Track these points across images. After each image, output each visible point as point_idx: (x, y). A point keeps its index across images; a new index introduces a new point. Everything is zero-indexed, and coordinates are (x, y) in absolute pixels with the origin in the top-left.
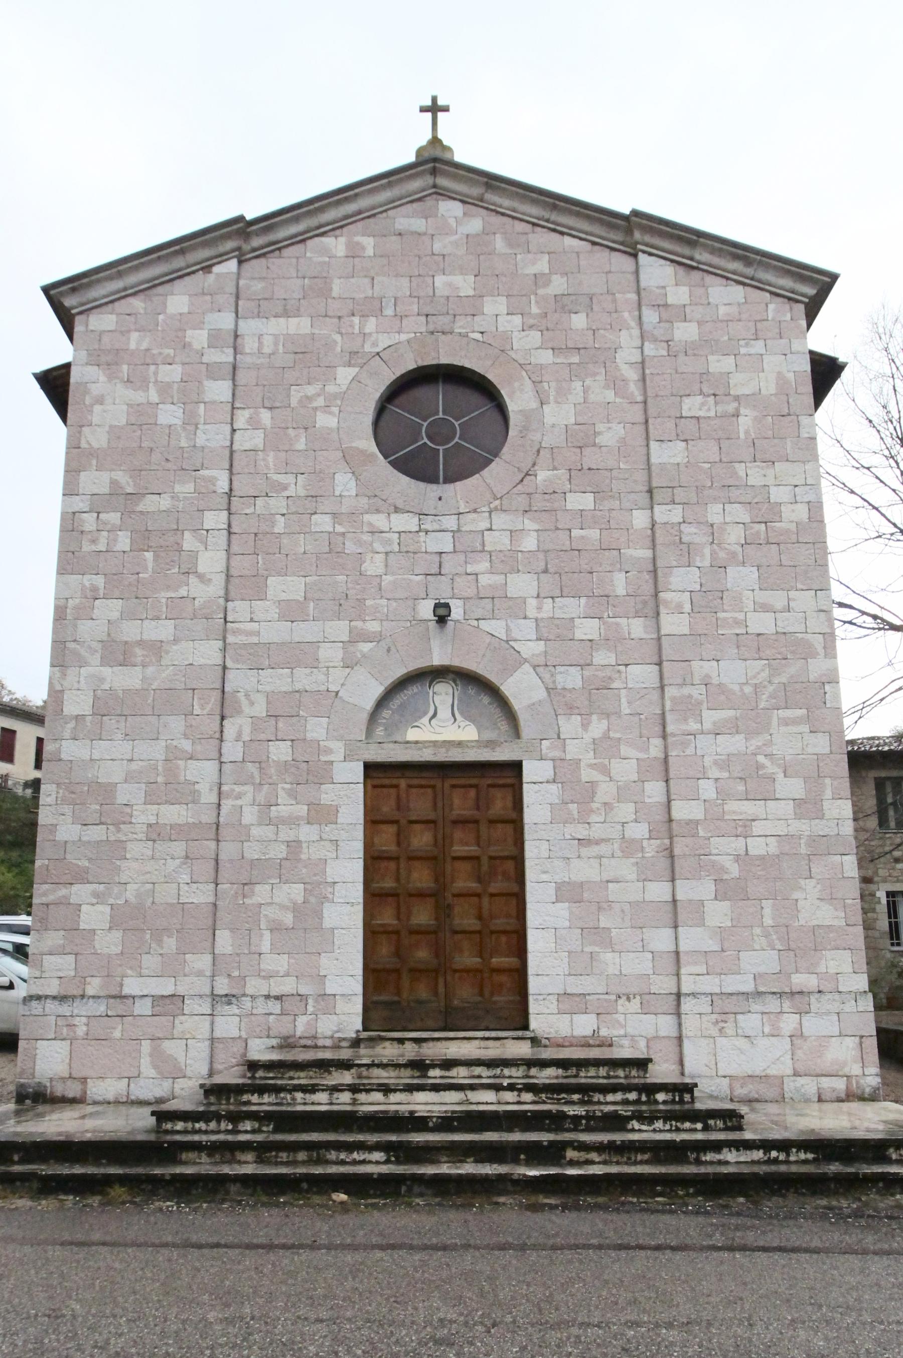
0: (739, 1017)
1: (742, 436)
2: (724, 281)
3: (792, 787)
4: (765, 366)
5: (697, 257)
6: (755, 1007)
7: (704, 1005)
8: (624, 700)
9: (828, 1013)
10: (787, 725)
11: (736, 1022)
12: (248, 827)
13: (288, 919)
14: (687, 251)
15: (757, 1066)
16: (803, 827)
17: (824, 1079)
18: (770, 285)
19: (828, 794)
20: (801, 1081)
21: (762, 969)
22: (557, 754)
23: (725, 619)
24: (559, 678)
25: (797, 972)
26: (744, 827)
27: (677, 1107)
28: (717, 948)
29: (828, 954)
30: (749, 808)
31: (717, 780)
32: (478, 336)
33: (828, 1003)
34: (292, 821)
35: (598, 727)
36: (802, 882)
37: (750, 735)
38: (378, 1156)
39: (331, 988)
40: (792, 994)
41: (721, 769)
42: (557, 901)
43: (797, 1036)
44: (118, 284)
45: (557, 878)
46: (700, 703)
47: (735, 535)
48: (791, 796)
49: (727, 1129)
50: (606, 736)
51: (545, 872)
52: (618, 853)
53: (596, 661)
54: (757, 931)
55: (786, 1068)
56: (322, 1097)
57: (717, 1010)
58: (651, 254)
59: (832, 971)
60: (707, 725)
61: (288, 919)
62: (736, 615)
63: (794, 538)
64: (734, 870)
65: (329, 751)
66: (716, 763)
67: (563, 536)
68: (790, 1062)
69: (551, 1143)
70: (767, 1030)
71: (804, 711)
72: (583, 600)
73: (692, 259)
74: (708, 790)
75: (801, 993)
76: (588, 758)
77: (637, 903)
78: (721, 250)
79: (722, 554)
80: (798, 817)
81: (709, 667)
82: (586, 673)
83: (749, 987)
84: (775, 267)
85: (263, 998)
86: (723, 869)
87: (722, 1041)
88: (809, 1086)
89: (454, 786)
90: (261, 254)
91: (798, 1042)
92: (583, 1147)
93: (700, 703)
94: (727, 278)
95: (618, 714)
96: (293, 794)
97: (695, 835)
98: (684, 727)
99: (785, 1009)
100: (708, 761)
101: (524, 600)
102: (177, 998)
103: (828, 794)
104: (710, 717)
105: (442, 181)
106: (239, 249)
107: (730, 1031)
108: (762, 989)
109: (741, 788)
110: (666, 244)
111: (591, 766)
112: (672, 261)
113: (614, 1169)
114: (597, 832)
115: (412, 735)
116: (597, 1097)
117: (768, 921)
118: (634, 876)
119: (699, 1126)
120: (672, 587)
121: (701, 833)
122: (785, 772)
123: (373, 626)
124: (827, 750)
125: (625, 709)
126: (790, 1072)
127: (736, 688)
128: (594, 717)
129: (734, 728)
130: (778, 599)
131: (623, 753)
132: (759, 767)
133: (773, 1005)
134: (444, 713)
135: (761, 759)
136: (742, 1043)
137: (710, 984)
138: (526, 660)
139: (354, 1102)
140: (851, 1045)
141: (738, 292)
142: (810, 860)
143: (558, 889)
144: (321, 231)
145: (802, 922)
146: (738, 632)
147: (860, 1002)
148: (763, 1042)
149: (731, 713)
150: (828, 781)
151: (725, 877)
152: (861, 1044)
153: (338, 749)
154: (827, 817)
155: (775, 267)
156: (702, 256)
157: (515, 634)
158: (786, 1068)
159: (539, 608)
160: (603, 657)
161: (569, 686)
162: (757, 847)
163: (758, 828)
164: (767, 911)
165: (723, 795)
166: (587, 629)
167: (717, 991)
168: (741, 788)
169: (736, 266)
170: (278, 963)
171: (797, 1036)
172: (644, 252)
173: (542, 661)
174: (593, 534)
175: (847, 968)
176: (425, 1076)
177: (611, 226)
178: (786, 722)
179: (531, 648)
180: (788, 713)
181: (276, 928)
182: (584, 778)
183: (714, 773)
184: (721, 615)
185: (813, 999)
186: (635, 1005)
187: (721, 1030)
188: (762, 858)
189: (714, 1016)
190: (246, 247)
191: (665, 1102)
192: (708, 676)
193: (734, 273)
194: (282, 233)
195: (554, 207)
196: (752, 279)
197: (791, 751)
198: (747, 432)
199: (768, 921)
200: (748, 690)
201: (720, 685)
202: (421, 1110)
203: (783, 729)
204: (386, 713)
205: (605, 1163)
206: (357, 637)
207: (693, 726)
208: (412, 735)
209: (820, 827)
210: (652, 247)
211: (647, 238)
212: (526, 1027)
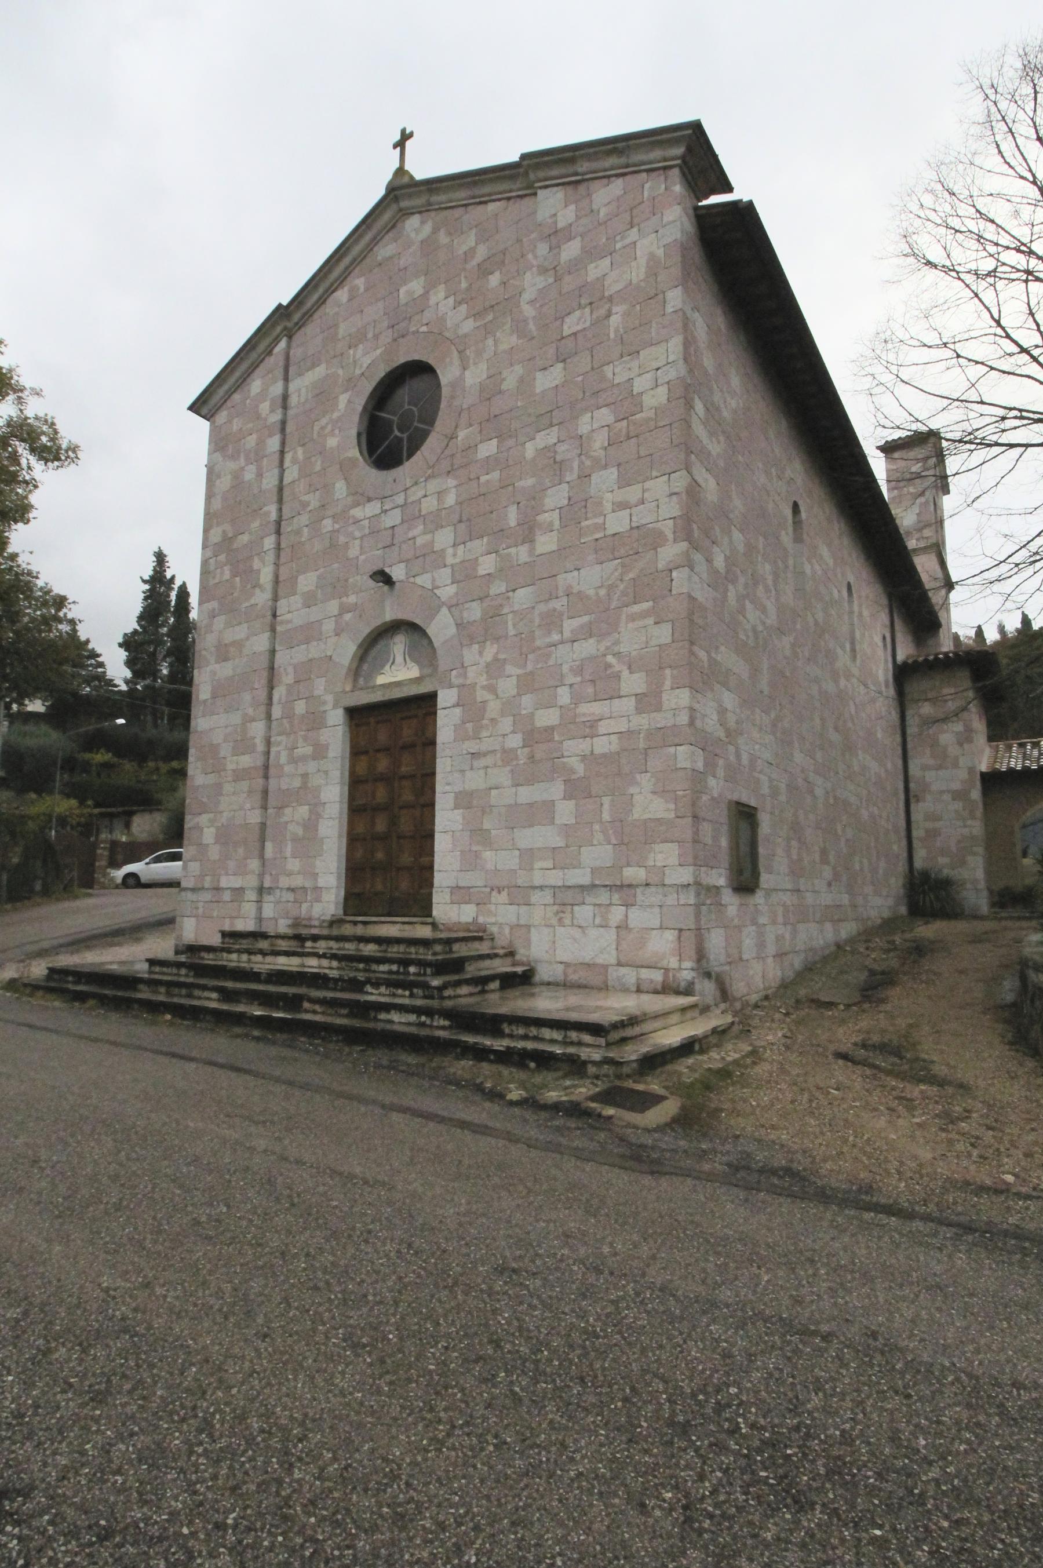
0: (576, 908)
1: (612, 336)
2: (605, 181)
3: (634, 683)
4: (638, 253)
5: (580, 170)
6: (589, 899)
7: (547, 897)
8: (510, 623)
9: (651, 906)
10: (633, 620)
11: (572, 912)
12: (282, 767)
13: (300, 832)
14: (571, 169)
15: (587, 955)
16: (642, 722)
17: (644, 970)
18: (644, 164)
19: (668, 683)
20: (623, 970)
21: (598, 863)
22: (461, 681)
23: (588, 527)
24: (465, 615)
25: (628, 865)
26: (590, 731)
27: (402, 977)
28: (562, 844)
29: (657, 847)
30: (596, 709)
31: (571, 685)
32: (424, 329)
33: (653, 896)
34: (304, 758)
35: (490, 651)
36: (638, 776)
37: (602, 636)
38: (214, 995)
39: (321, 882)
40: (622, 886)
41: (575, 675)
42: (456, 808)
43: (623, 927)
44: (226, 387)
45: (457, 789)
46: (561, 614)
47: (600, 440)
48: (634, 692)
49: (425, 997)
50: (496, 659)
51: (448, 784)
52: (500, 763)
53: (492, 592)
54: (597, 827)
55: (610, 957)
56: (234, 956)
57: (558, 901)
58: (546, 187)
59: (659, 864)
60: (567, 634)
61: (300, 832)
62: (596, 520)
63: (652, 424)
64: (580, 769)
65: (324, 703)
66: (571, 669)
67: (474, 484)
68: (614, 952)
69: (295, 995)
70: (598, 921)
71: (651, 603)
72: (485, 539)
73: (576, 174)
74: (564, 696)
75: (630, 886)
76: (483, 680)
77: (510, 806)
78: (596, 153)
79: (588, 463)
80: (639, 711)
81: (571, 578)
82: (485, 605)
83: (586, 880)
84: (643, 145)
85: (184, 884)
86: (572, 771)
87: (560, 930)
88: (630, 976)
89: (402, 719)
90: (300, 325)
91: (623, 932)
92: (311, 1000)
93: (561, 614)
94: (609, 177)
95: (506, 637)
96: (305, 739)
97: (551, 740)
98: (548, 640)
99: (614, 901)
100: (565, 668)
101: (443, 550)
102: (241, 890)
103: (668, 683)
104: (570, 626)
105: (404, 204)
106: (285, 328)
107: (567, 921)
108: (597, 882)
109: (590, 690)
110: (555, 172)
111: (483, 688)
112: (557, 185)
113: (329, 1020)
114: (484, 747)
115: (381, 680)
116: (374, 967)
117: (606, 816)
118: (509, 782)
119: (407, 993)
120: (546, 508)
121: (557, 738)
122: (630, 668)
123: (352, 599)
124: (669, 640)
125: (512, 632)
126: (614, 961)
127: (591, 592)
128: (488, 643)
129: (588, 631)
130: (633, 493)
131: (507, 673)
132: (608, 666)
133: (603, 897)
134: (399, 659)
135: (610, 659)
136: (576, 933)
137: (555, 878)
138: (443, 603)
139: (249, 961)
140: (671, 938)
141: (617, 186)
142: (646, 754)
143: (456, 798)
144: (331, 290)
145: (636, 816)
146: (597, 536)
147: (682, 897)
148: (593, 933)
149: (586, 619)
150: (668, 672)
151: (573, 777)
152: (679, 937)
153: (329, 698)
154: (665, 707)
155: (643, 145)
156: (583, 166)
157: (438, 583)
158: (610, 957)
159: (455, 555)
160: (498, 588)
161: (472, 619)
162: (602, 745)
163: (603, 727)
164: (606, 807)
165: (578, 699)
166: (487, 565)
167: (560, 884)
168: (590, 690)
169: (613, 160)
170: (294, 865)
171: (623, 927)
172: (541, 188)
173: (454, 601)
174: (495, 475)
175: (674, 860)
176: (303, 947)
177: (512, 178)
178: (632, 618)
179: (447, 592)
180: (636, 608)
181: (295, 840)
182: (479, 699)
183: (571, 679)
184: (584, 523)
185: (639, 891)
186: (504, 897)
187: (560, 919)
188: (604, 756)
189: (556, 907)
190: (289, 325)
191: (414, 974)
192: (570, 587)
193: (612, 169)
194: (309, 304)
195: (475, 183)
196: (627, 166)
197: (636, 646)
198: (617, 331)
199: (606, 816)
200: (602, 592)
201: (579, 592)
202: (257, 968)
203: (630, 625)
204: (365, 667)
205: (323, 1013)
206: (344, 609)
207: (556, 637)
208: (381, 680)
209: (661, 720)
210: (546, 180)
211: (541, 174)
212: (430, 916)
